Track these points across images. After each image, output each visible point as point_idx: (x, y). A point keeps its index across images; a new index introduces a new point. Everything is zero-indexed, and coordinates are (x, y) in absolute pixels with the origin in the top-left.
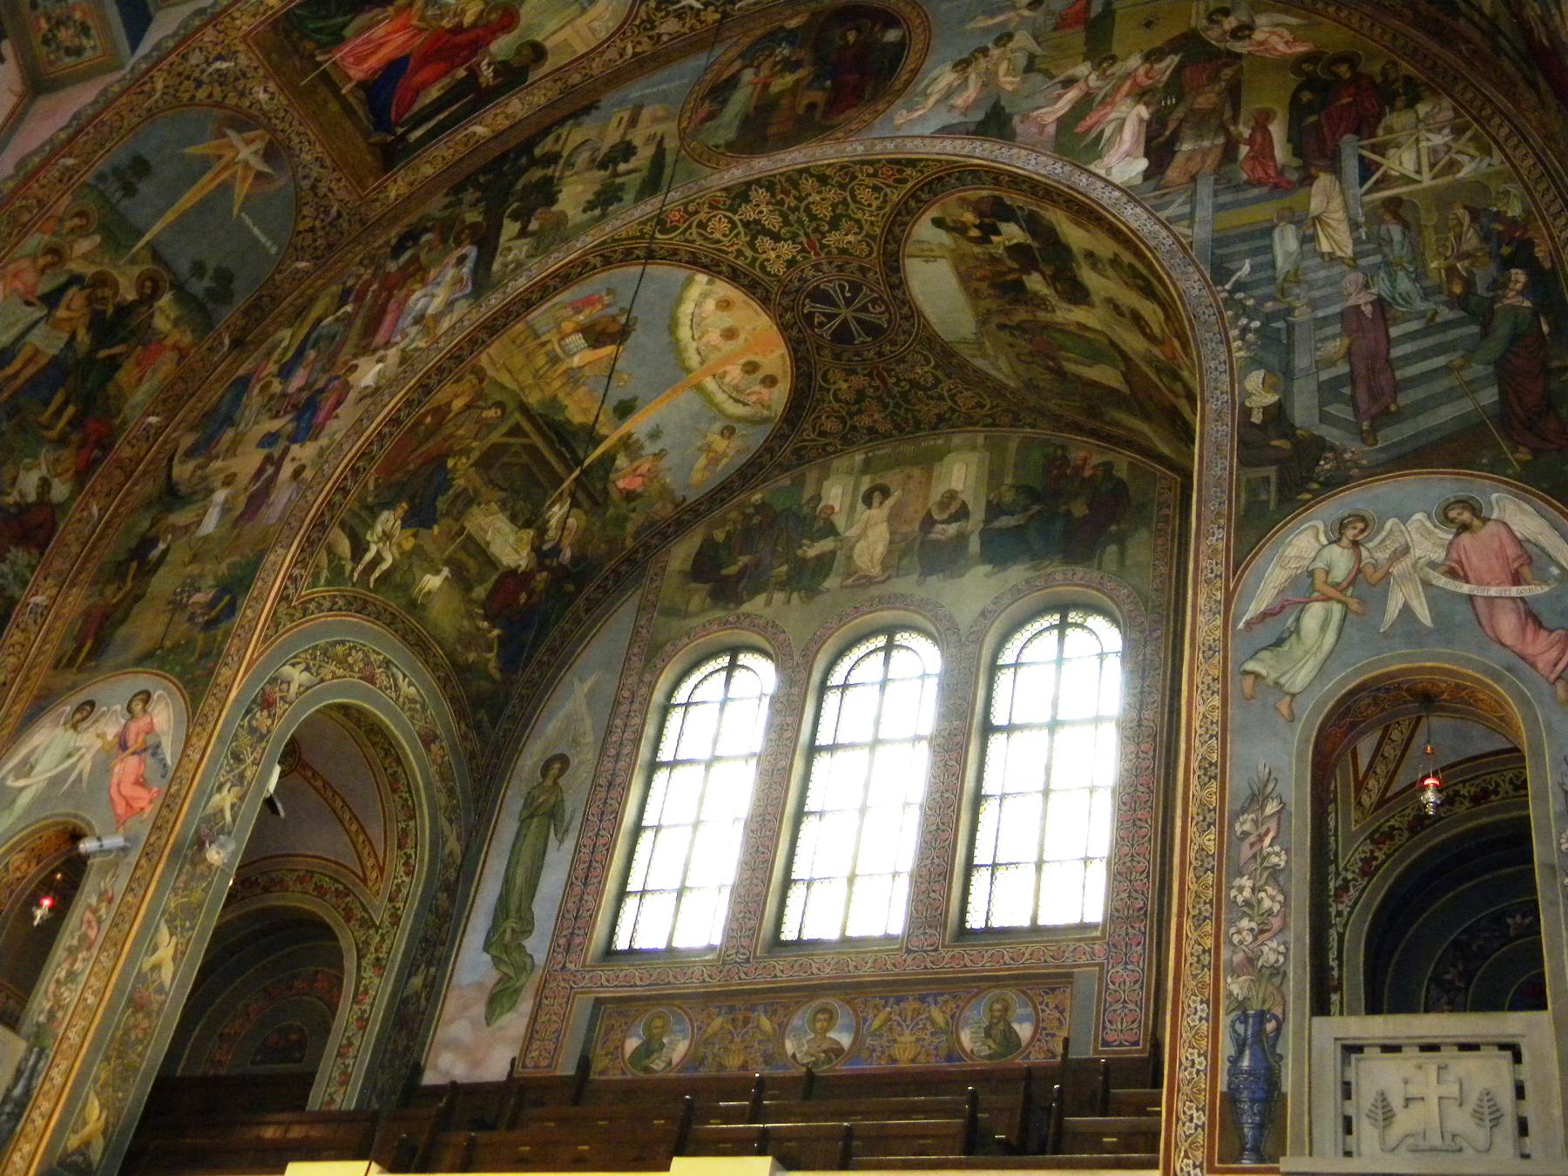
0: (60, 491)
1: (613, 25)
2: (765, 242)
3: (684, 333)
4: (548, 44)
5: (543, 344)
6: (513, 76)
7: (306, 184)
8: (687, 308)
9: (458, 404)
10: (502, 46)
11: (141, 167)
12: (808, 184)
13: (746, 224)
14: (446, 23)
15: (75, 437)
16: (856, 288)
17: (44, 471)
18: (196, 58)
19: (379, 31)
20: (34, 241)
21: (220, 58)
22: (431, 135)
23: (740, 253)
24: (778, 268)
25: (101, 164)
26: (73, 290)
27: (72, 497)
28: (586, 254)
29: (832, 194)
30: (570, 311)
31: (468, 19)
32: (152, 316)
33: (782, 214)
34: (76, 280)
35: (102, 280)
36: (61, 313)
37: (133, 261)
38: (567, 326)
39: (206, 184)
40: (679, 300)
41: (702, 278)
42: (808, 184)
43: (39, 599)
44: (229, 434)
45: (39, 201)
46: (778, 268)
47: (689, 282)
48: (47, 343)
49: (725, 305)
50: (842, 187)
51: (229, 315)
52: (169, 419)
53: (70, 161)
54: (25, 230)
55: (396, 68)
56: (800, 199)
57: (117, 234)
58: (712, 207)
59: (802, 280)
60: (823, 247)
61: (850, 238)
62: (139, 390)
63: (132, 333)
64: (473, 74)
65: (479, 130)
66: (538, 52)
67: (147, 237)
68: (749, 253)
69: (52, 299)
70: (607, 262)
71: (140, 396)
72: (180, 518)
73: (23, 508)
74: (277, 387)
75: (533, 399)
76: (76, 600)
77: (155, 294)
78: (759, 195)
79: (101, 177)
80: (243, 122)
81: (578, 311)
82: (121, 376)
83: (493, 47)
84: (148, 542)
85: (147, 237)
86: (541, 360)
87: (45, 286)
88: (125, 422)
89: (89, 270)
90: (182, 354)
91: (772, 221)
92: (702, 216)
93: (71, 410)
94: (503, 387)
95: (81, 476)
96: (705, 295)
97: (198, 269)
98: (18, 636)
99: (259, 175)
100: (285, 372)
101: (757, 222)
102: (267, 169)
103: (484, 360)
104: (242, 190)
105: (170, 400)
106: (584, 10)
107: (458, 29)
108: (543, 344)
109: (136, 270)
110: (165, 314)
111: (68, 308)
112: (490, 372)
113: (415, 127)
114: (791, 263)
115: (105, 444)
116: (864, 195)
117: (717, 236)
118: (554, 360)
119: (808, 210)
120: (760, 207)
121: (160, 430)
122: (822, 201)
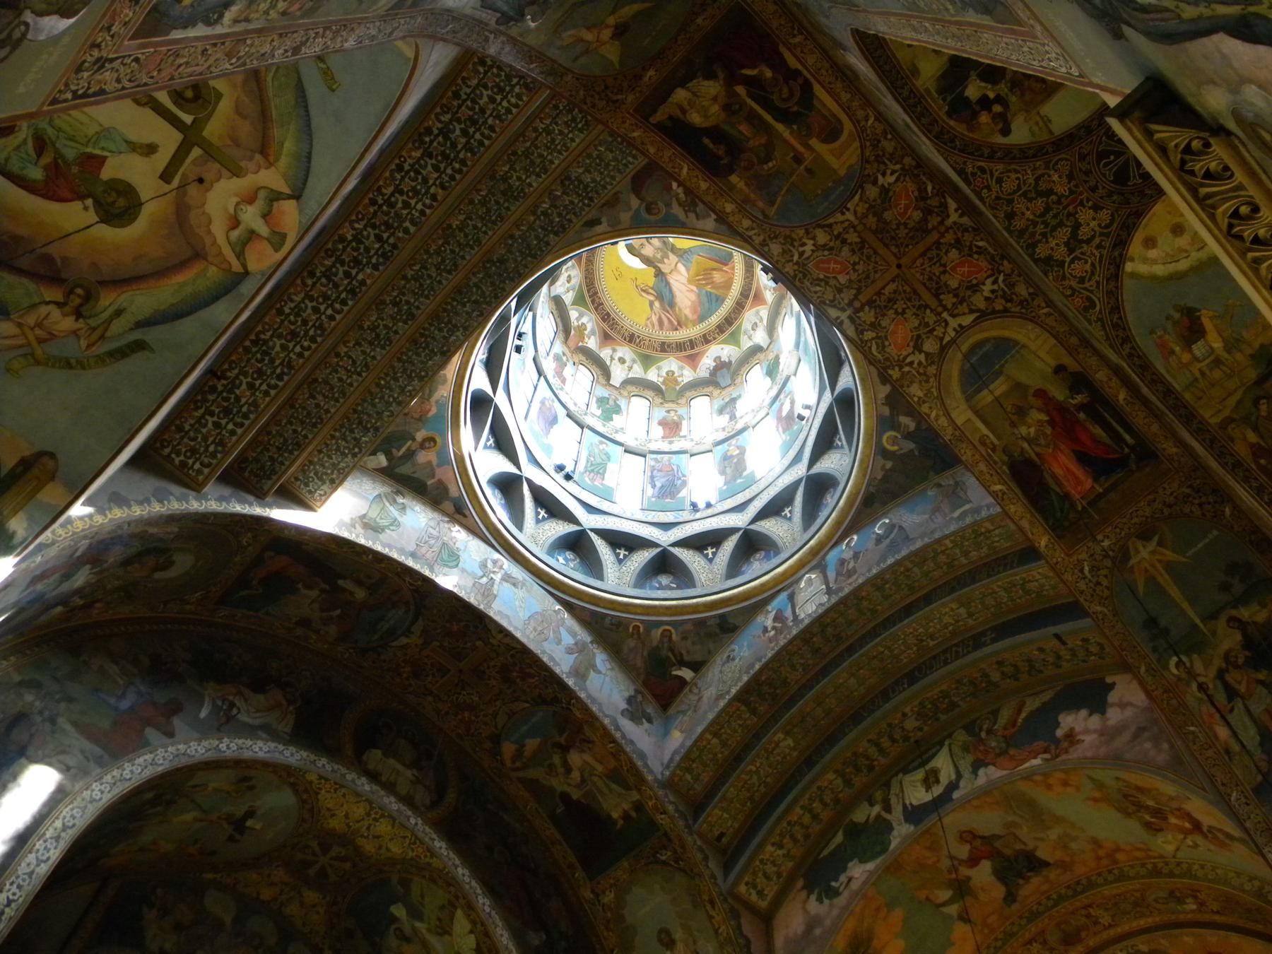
1: (1030, 326)
2: (1084, 232)
3: (1183, 265)
4: (1053, 363)
5: (1203, 374)
6: (1079, 382)
7: (1166, 511)
8: (1159, 270)
9: (1252, 437)
10: (1059, 393)
11: (1151, 623)
12: (1018, 223)
13: (1071, 251)
14: (1049, 431)
16: (1102, 155)
18: (1082, 585)
19: (1059, 472)
20: (1190, 701)
21: (1082, 571)
22: (1129, 428)
23: (1098, 247)
24: (1104, 216)
26: (1228, 677)
28: (1122, 357)
29: (1020, 205)
30: (1172, 359)
31: (1043, 417)
32: (1255, 623)
33: (1054, 229)
34: (1221, 674)
36: (1242, 688)
37: (1214, 633)
38: (1186, 357)
39: (1165, 580)
40: (1153, 278)
41: (1129, 267)
42: (1018, 223)
45: (1165, 692)
46: (1104, 216)
47: (1133, 275)
49: (1150, 242)
50: (1010, 202)
53: (1143, 669)
55: (1083, 458)
56: (1035, 224)
57: (1194, 643)
58: (1064, 278)
59: (1110, 194)
60: (1071, 192)
61: (1055, 178)
64: (1081, 407)
65: (1121, 397)
66: (1059, 369)
67: (1198, 621)
68: (1097, 240)
69: (1232, 694)
70: (1127, 339)
75: (1252, 374)
78: (1042, 251)
79: (1155, 649)
80: (1125, 555)
81: (1173, 352)
83: (1061, 397)
85: (1198, 621)
86: (1217, 374)
89: (1218, 663)
91: (1064, 234)
92: (1074, 284)
94: (1239, 402)
96: (1145, 260)
99: (1160, 544)
101: (1067, 244)
102: (1156, 538)
103: (1214, 421)
104: (1170, 555)
106: (1024, 346)
107: (1051, 422)
108: (1203, 374)
111: (1240, 683)
112: (1226, 413)
113: (1124, 440)
114: (1096, 208)
116: (1009, 185)
117: (1088, 267)
118: (1218, 362)
119: (1042, 215)
120: (1055, 246)
122: (1028, 211)
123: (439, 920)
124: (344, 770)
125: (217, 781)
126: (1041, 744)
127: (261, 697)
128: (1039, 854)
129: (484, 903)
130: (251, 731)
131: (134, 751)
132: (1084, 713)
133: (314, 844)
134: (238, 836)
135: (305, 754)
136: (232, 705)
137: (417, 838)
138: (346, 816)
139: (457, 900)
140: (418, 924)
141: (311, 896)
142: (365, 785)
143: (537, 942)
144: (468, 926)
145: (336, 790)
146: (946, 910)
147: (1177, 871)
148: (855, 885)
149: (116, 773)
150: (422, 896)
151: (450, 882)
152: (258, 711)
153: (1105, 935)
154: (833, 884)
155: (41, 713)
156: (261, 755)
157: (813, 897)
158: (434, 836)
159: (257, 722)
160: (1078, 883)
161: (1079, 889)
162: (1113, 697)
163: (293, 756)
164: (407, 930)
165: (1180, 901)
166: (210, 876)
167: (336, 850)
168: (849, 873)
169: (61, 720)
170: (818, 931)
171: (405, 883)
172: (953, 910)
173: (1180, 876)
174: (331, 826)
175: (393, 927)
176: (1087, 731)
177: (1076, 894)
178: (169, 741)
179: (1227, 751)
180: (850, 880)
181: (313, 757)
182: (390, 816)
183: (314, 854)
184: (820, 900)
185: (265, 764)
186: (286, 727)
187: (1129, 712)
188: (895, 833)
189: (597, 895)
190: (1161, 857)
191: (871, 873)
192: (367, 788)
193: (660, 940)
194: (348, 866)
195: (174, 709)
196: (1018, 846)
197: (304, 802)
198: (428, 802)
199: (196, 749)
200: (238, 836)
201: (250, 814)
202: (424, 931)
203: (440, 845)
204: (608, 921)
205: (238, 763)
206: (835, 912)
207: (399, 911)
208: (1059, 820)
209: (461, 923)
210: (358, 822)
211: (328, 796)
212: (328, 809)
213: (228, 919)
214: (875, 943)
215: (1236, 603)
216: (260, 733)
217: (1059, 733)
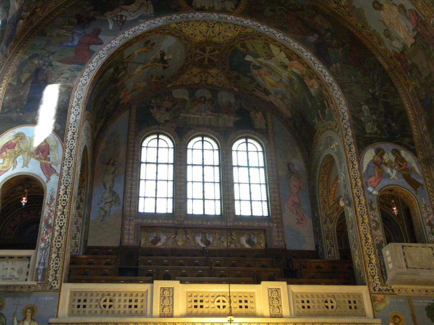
123: (266, 53)
124: (186, 15)
125: (136, 49)
127: (133, 5)
129: (279, 36)
130: (135, 22)
131: (90, 58)
133: (198, 51)
134: (166, 65)
135: (164, 18)
136: (122, 16)
137: (235, 25)
138: (201, 33)
139: (268, 41)
140: (259, 60)
141: (213, 71)
142: (199, 15)
143: (314, 40)
144: (278, 49)
145: (187, 25)
149: (87, 70)
150: (254, 47)
151: (260, 35)
152: (135, 12)
155: (44, 65)
156: (145, 29)
158: (243, 19)
159: (137, 16)
163: (159, 22)
164: (258, 65)
166: (169, 86)
167: (208, 49)
169: (53, 63)
171: (244, 46)
174: (198, 40)
175: (251, 67)
178: (102, 46)
181: (169, 17)
182: (217, 22)
183: (201, 55)
185: (149, 32)
186: (151, 10)
189: (338, 4)
192: (201, 16)
193: (376, 9)
194: (217, 52)
195: (97, 32)
197: (179, 37)
198: (234, 7)
199: (116, 43)
200: (166, 65)
201: (163, 54)
202: (264, 61)
203: (248, 22)
204: (349, 13)
205: (137, 38)
207: (249, 58)
209: (275, 50)
210: (207, 32)
211: (187, 29)
212: (192, 34)
213: (187, 98)
216: (139, 21)
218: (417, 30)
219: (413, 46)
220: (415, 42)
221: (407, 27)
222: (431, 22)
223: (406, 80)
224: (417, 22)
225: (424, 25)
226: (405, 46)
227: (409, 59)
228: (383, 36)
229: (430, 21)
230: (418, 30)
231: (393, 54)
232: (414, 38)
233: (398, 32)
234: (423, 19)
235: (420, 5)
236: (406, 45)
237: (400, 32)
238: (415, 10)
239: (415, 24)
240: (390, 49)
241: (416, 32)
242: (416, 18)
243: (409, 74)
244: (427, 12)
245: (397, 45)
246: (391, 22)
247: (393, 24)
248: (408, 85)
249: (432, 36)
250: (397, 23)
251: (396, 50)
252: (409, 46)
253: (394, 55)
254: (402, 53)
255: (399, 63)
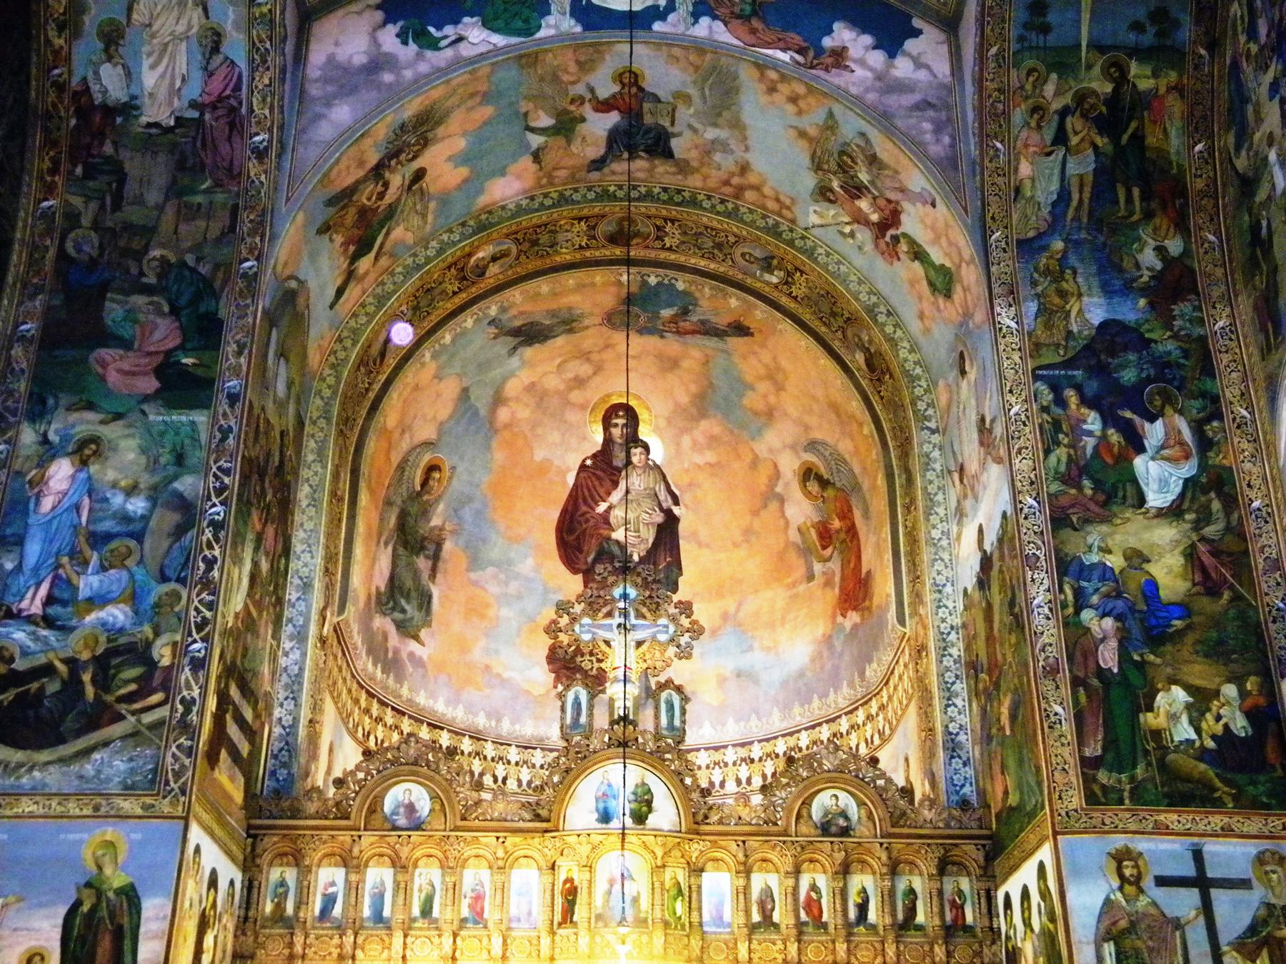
0: (1175, 246)
15: (1154, 205)
17: (1152, 243)
20: (1018, 116)
25: (1013, 34)
26: (1069, 120)
27: (1187, 241)
32: (1134, 86)
34: (1064, 113)
35: (1081, 97)
36: (1074, 140)
37: (1089, 67)
43: (1221, 324)
44: (1250, 108)
45: (999, 90)
48: (1082, 166)
51: (1187, 32)
52: (1211, 137)
53: (994, 50)
54: (1006, 114)
57: (1063, 61)
62: (1171, 138)
63: (1132, 109)
67: (1084, 44)
69: (1061, 138)
71: (1175, 142)
72: (1261, 195)
73: (1157, 277)
74: (1254, 48)
76: (1245, 305)
77: (1123, 72)
79: (1021, 39)
82: (1151, 141)
84: (1255, 228)
85: (1084, 44)
87: (1049, 134)
88: (1180, 166)
89: (1067, 99)
90: (1178, 89)
93: (1136, 192)
95: (1181, 225)
97: (1137, 27)
98: (1225, 358)
100: (1252, 34)
105: (1198, 126)
109: (1097, 70)
110: (1141, 76)
111: (1076, 133)
115: (1178, 189)
121: (1210, 150)
126: (797, 39)
128: (674, 143)
132: (867, 39)
146: (530, 136)
147: (798, 243)
148: (465, 50)
153: (663, 255)
154: (432, 30)
157: (392, 29)
160: (679, 192)
161: (677, 198)
162: (910, 45)
165: (769, 268)
168: (461, 30)
170: (388, 77)
172: (536, 140)
173: (799, 250)
176: (862, 62)
177: (670, 201)
179: (1018, 190)
180: (460, 39)
184: (403, 37)
187: (922, 75)
188: (551, 20)
190: (793, 221)
191: (497, 50)
196: (666, 123)
206: (423, 68)
208: (737, 125)
214: (440, 131)
215: (1137, 53)
217: (827, 42)
218: (202, 114)
219: (154, 131)
220: (170, 130)
221: (183, 80)
222: (257, 139)
223: (54, 171)
224: (220, 99)
225: (232, 125)
226: (129, 108)
227: (115, 143)
228: (90, 22)
229: (257, 134)
230: (207, 116)
231: (75, 81)
232: (178, 119)
233: (146, 63)
234: (244, 110)
235: (267, 81)
236: (137, 108)
237: (153, 67)
238: (240, 76)
239: (213, 98)
240: (80, 70)
241: (196, 114)
242: (228, 92)
243: (79, 170)
244: (267, 112)
245: (110, 83)
246: (150, 25)
247: (153, 36)
248: (49, 190)
249: (231, 162)
250: (166, 45)
251: (95, 88)
252: (144, 120)
253: (76, 93)
254: (110, 111)
255: (73, 122)
